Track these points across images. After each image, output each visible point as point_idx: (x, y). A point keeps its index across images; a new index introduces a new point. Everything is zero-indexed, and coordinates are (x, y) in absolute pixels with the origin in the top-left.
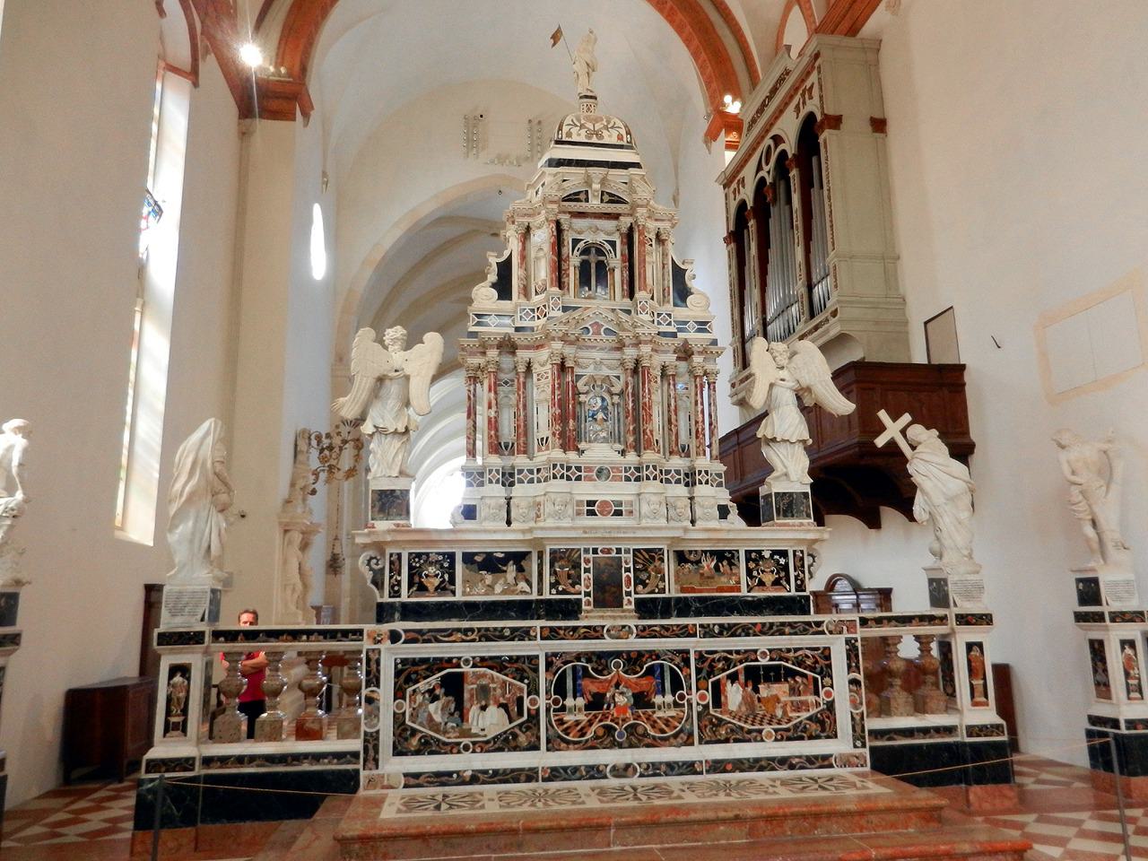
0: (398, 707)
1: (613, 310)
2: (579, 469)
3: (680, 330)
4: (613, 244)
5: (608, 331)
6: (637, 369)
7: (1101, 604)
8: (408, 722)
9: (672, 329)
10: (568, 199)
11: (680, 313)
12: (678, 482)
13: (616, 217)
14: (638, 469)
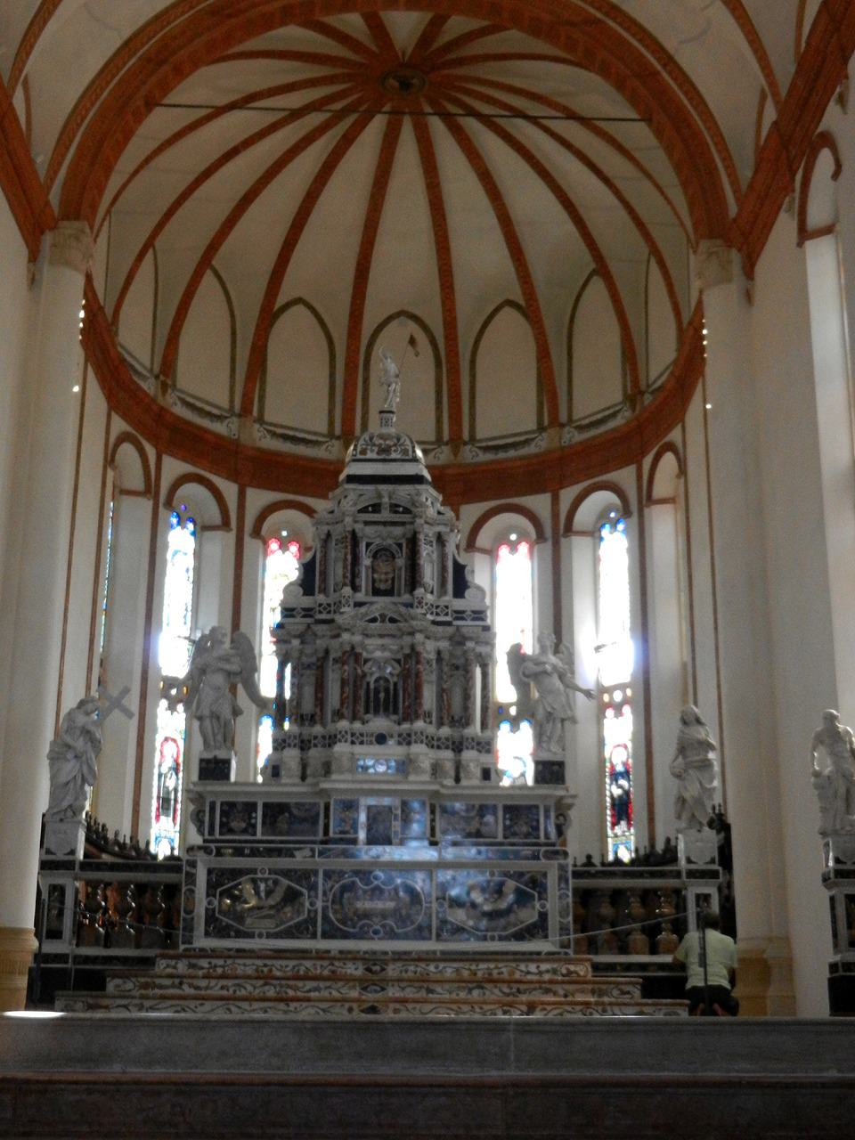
0: (209, 903)
1: (395, 604)
2: (362, 735)
3: (457, 619)
4: (400, 546)
5: (392, 620)
6: (414, 654)
8: (217, 915)
9: (448, 619)
10: (364, 510)
11: (458, 604)
12: (447, 748)
13: (403, 524)
14: (409, 735)
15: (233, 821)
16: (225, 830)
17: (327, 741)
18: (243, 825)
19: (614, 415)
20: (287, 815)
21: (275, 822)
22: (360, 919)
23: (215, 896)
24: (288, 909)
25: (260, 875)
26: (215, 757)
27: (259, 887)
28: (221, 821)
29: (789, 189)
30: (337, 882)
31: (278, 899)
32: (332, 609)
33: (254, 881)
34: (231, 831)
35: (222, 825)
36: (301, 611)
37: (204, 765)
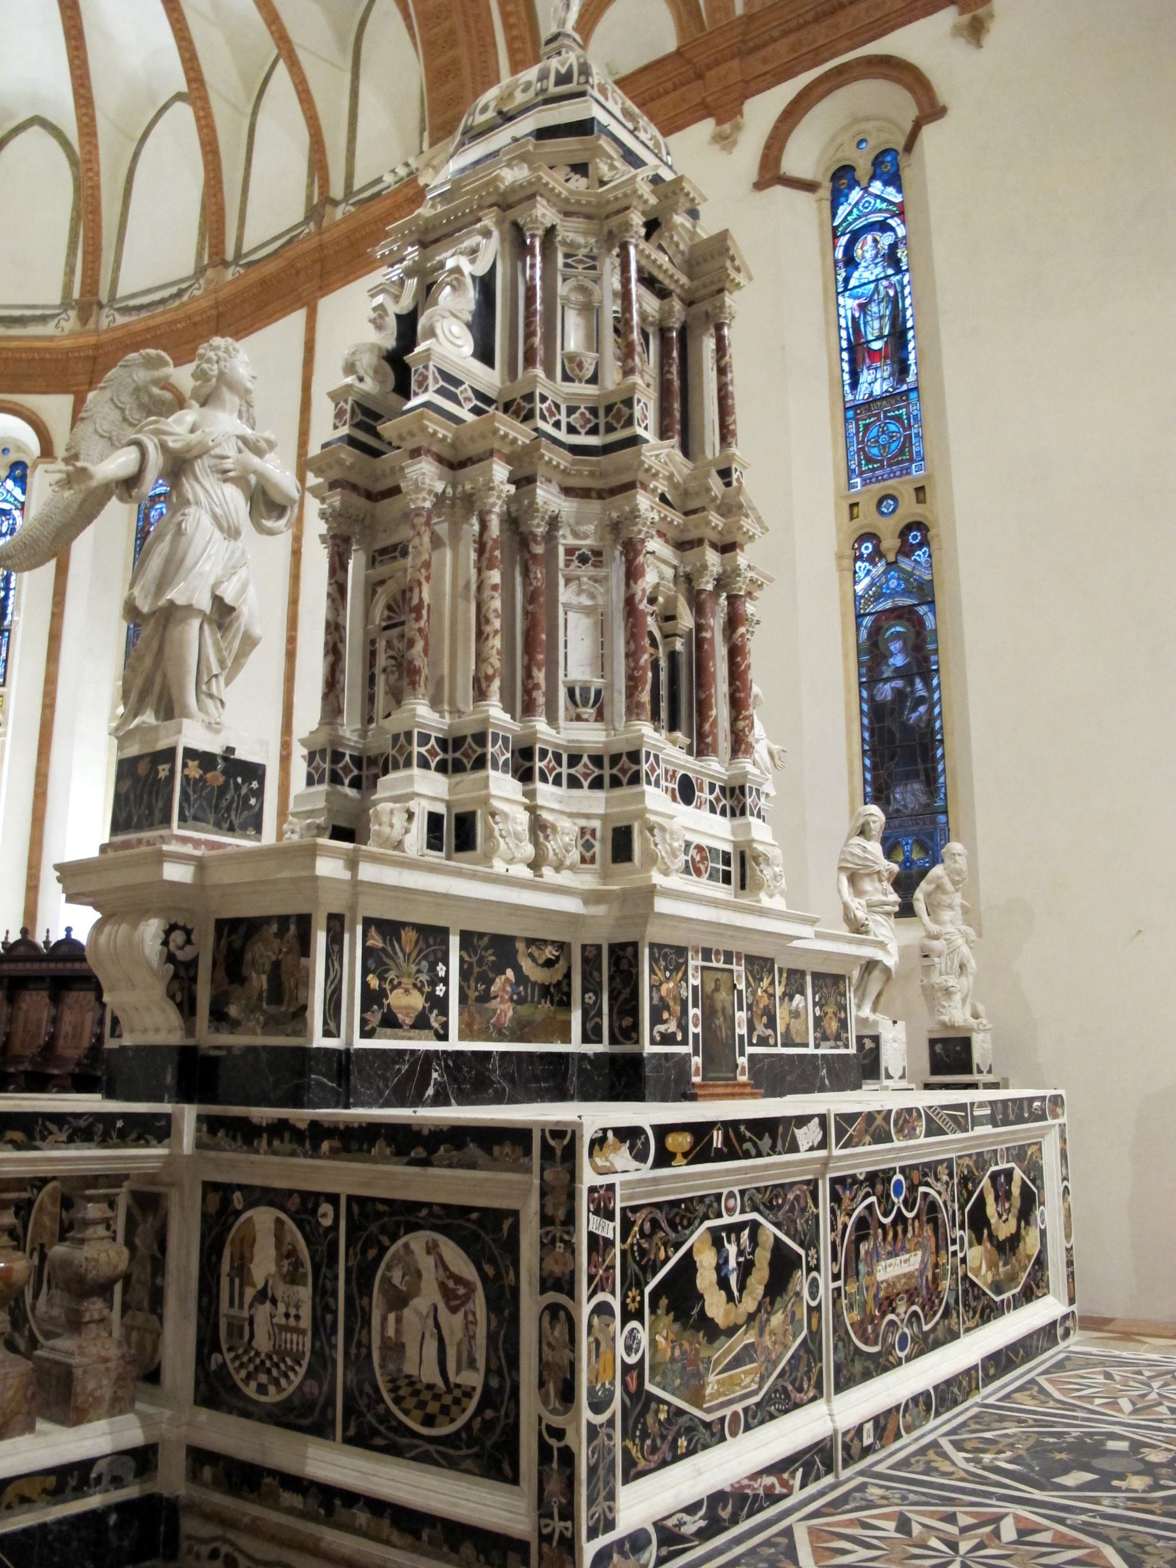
7: (970, 1072)
15: (394, 988)
16: (375, 1018)
17: (607, 772)
18: (417, 1001)
19: (43, 319)
20: (510, 973)
21: (486, 997)
22: (884, 1315)
23: (639, 1315)
24: (777, 1319)
25: (726, 1220)
26: (230, 750)
27: (726, 1261)
28: (365, 985)
29: (725, 110)
30: (850, 1215)
31: (760, 1290)
32: (602, 421)
33: (717, 1239)
34: (390, 1022)
35: (371, 998)
36: (470, 394)
37: (194, 771)
